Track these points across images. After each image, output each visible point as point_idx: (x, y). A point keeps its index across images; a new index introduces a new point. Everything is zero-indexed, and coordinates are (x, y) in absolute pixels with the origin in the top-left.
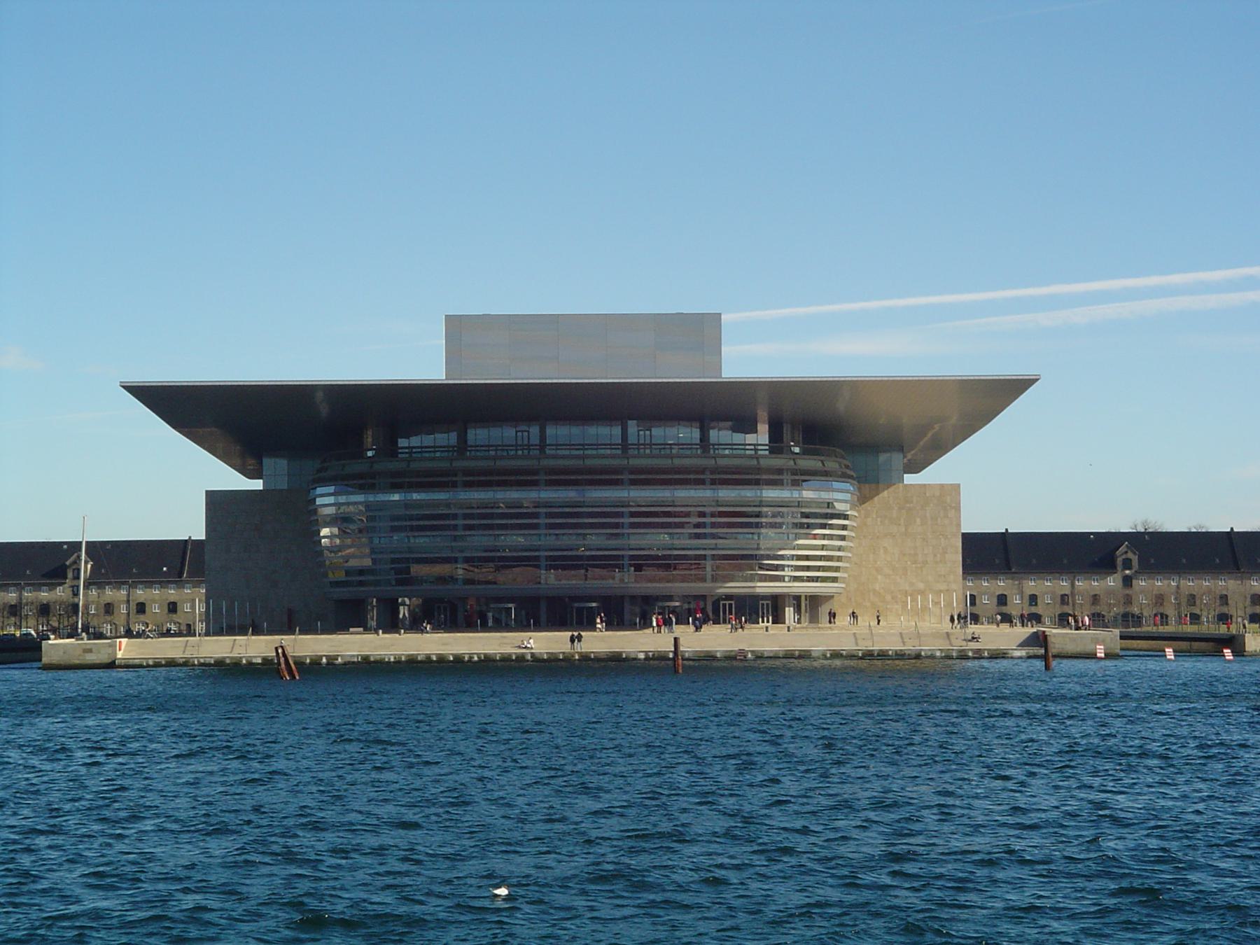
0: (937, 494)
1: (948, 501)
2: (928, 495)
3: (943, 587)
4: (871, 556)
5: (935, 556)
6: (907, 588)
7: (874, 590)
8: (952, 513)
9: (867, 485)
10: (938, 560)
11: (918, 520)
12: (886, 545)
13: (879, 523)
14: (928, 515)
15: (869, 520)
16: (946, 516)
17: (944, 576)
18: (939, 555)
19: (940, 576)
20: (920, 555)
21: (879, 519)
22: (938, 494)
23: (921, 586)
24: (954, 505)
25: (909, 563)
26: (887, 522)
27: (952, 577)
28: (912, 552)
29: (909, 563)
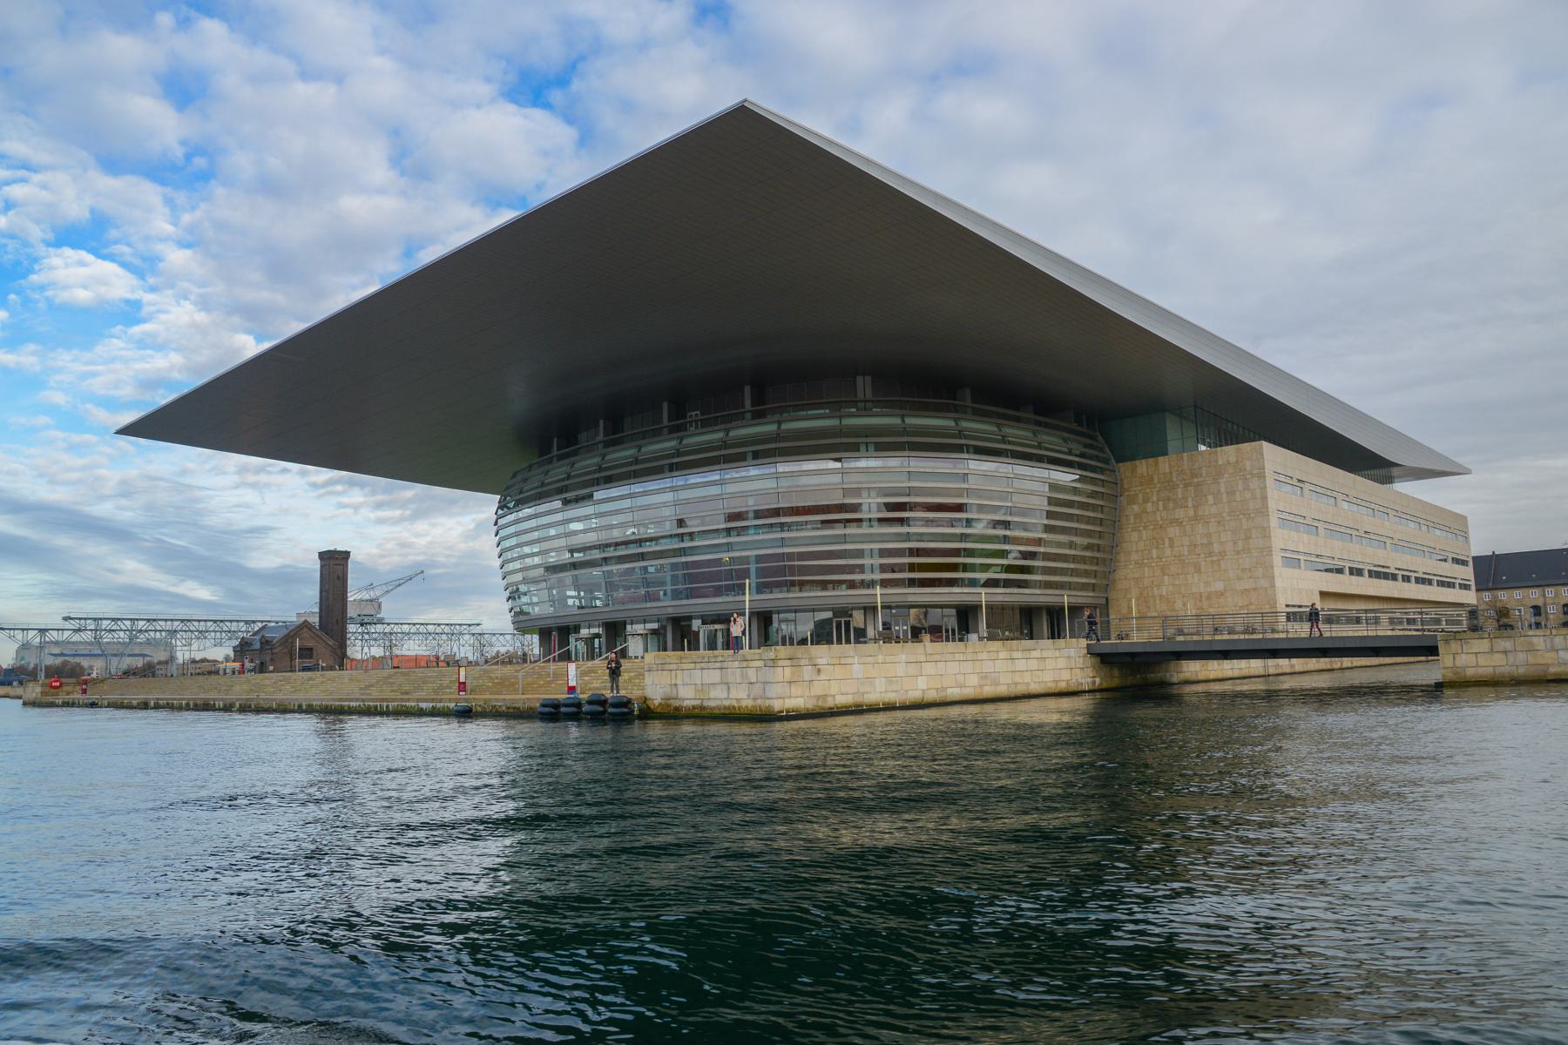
0: (1233, 459)
1: (1248, 468)
2: (1220, 462)
3: (1247, 584)
4: (1154, 551)
5: (1235, 543)
6: (1202, 589)
7: (1161, 596)
8: (1254, 484)
9: (1143, 461)
10: (1240, 548)
11: (1210, 498)
12: (1172, 535)
13: (1161, 508)
14: (1223, 490)
15: (1149, 507)
16: (1247, 488)
17: (1250, 570)
18: (1240, 543)
19: (1243, 570)
20: (1215, 545)
21: (1161, 503)
22: (1235, 460)
23: (1219, 586)
24: (1255, 472)
25: (1202, 556)
26: (1171, 504)
27: (1260, 571)
28: (1206, 542)
29: (1202, 556)
